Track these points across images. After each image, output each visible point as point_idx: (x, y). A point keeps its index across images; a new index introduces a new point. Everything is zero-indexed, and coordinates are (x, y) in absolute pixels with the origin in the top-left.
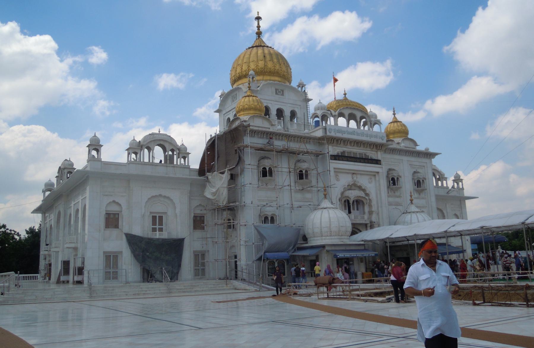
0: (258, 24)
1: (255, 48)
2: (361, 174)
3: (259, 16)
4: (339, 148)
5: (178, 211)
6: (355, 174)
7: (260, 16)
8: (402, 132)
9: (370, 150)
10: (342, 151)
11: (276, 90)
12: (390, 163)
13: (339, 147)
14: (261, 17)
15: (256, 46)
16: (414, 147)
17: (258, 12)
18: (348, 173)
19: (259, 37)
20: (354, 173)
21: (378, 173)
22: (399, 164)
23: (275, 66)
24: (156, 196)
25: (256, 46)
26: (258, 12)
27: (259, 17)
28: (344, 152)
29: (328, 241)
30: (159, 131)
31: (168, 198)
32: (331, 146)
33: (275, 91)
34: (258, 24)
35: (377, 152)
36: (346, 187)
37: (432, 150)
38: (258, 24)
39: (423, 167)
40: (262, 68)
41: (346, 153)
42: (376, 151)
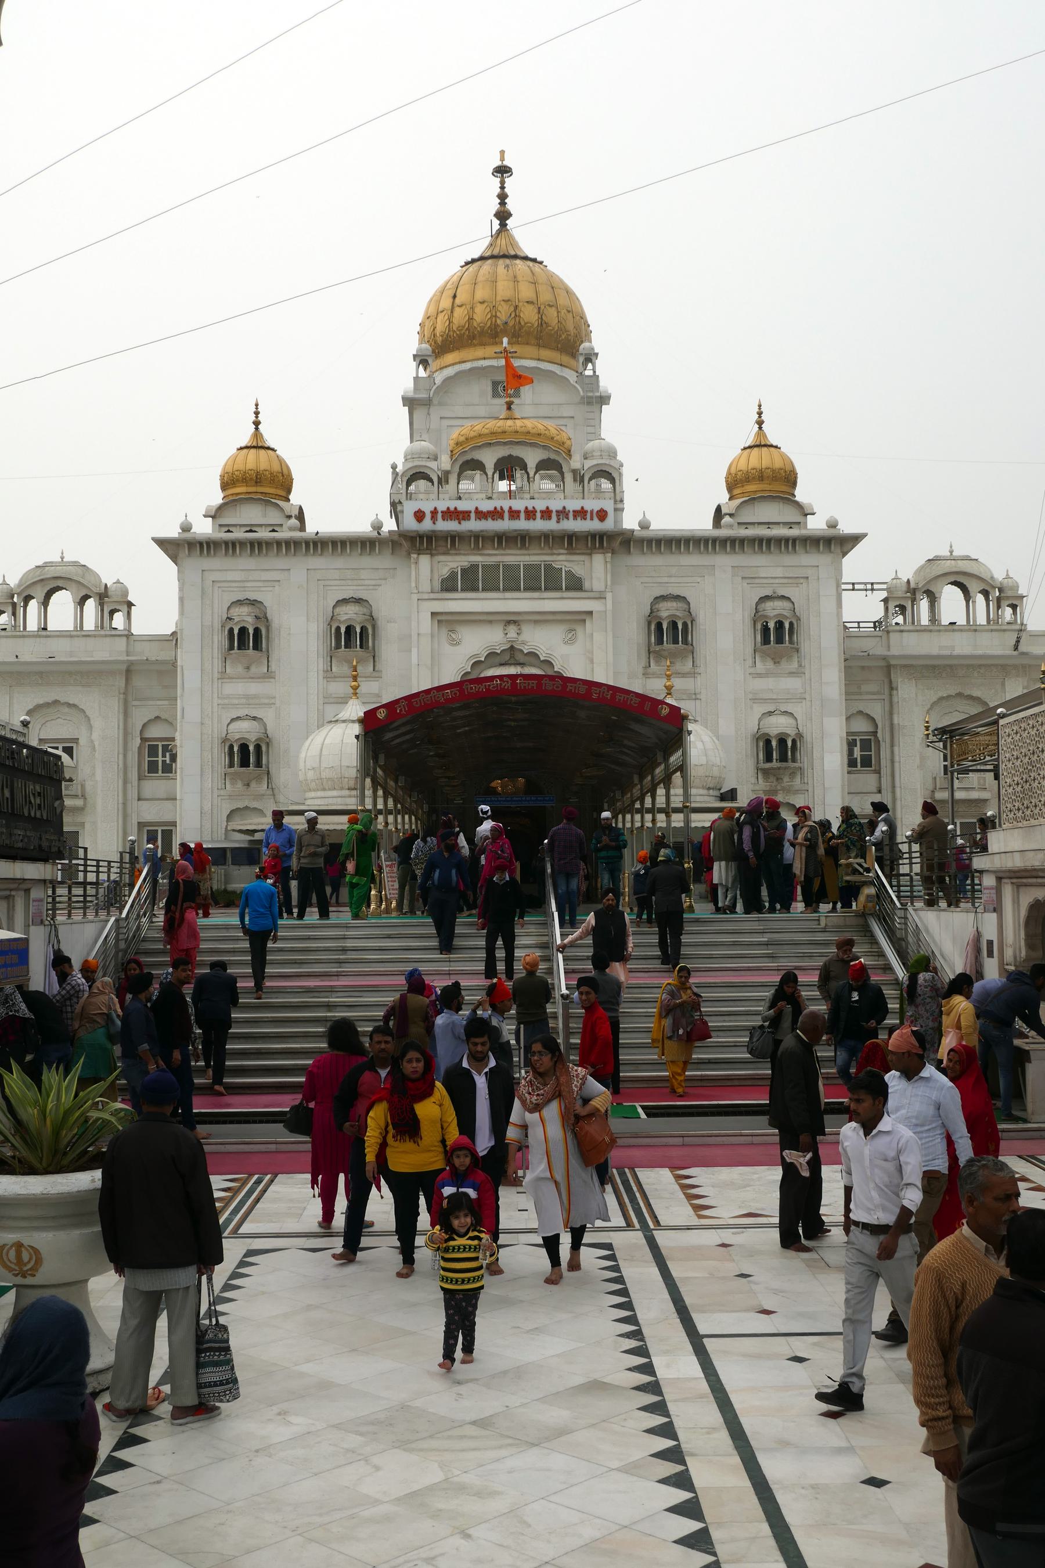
0: (502, 188)
1: (490, 261)
2: (536, 622)
3: (505, 163)
4: (458, 558)
5: (95, 736)
6: (515, 622)
7: (506, 163)
8: (754, 478)
9: (565, 552)
10: (466, 564)
11: (495, 384)
12: (666, 580)
13: (456, 554)
14: (510, 168)
15: (492, 257)
16: (797, 518)
17: (502, 153)
18: (490, 622)
19: (503, 225)
20: (512, 620)
21: (590, 613)
22: (699, 579)
23: (496, 316)
24: (47, 705)
25: (492, 257)
26: (502, 153)
27: (505, 167)
28: (474, 567)
29: (335, 801)
30: (62, 558)
31: (74, 705)
32: (429, 556)
33: (489, 389)
34: (500, 188)
35: (590, 554)
36: (483, 659)
37: (846, 528)
38: (502, 188)
39: (802, 581)
40: (460, 328)
41: (480, 569)
42: (589, 551)
